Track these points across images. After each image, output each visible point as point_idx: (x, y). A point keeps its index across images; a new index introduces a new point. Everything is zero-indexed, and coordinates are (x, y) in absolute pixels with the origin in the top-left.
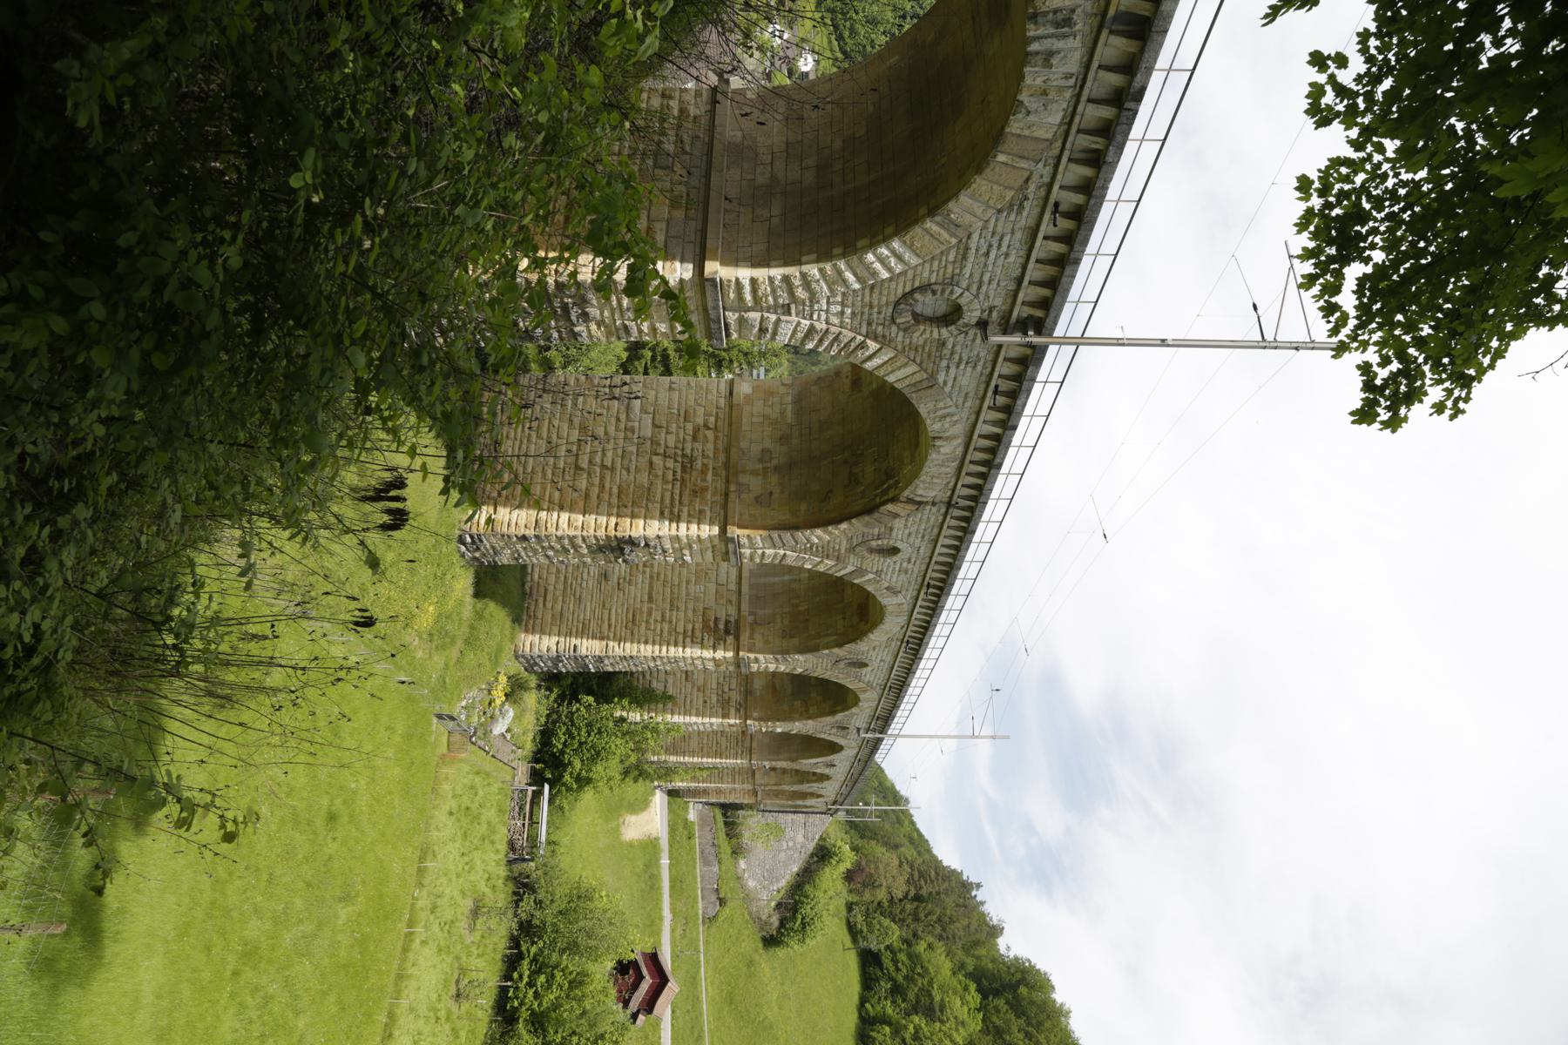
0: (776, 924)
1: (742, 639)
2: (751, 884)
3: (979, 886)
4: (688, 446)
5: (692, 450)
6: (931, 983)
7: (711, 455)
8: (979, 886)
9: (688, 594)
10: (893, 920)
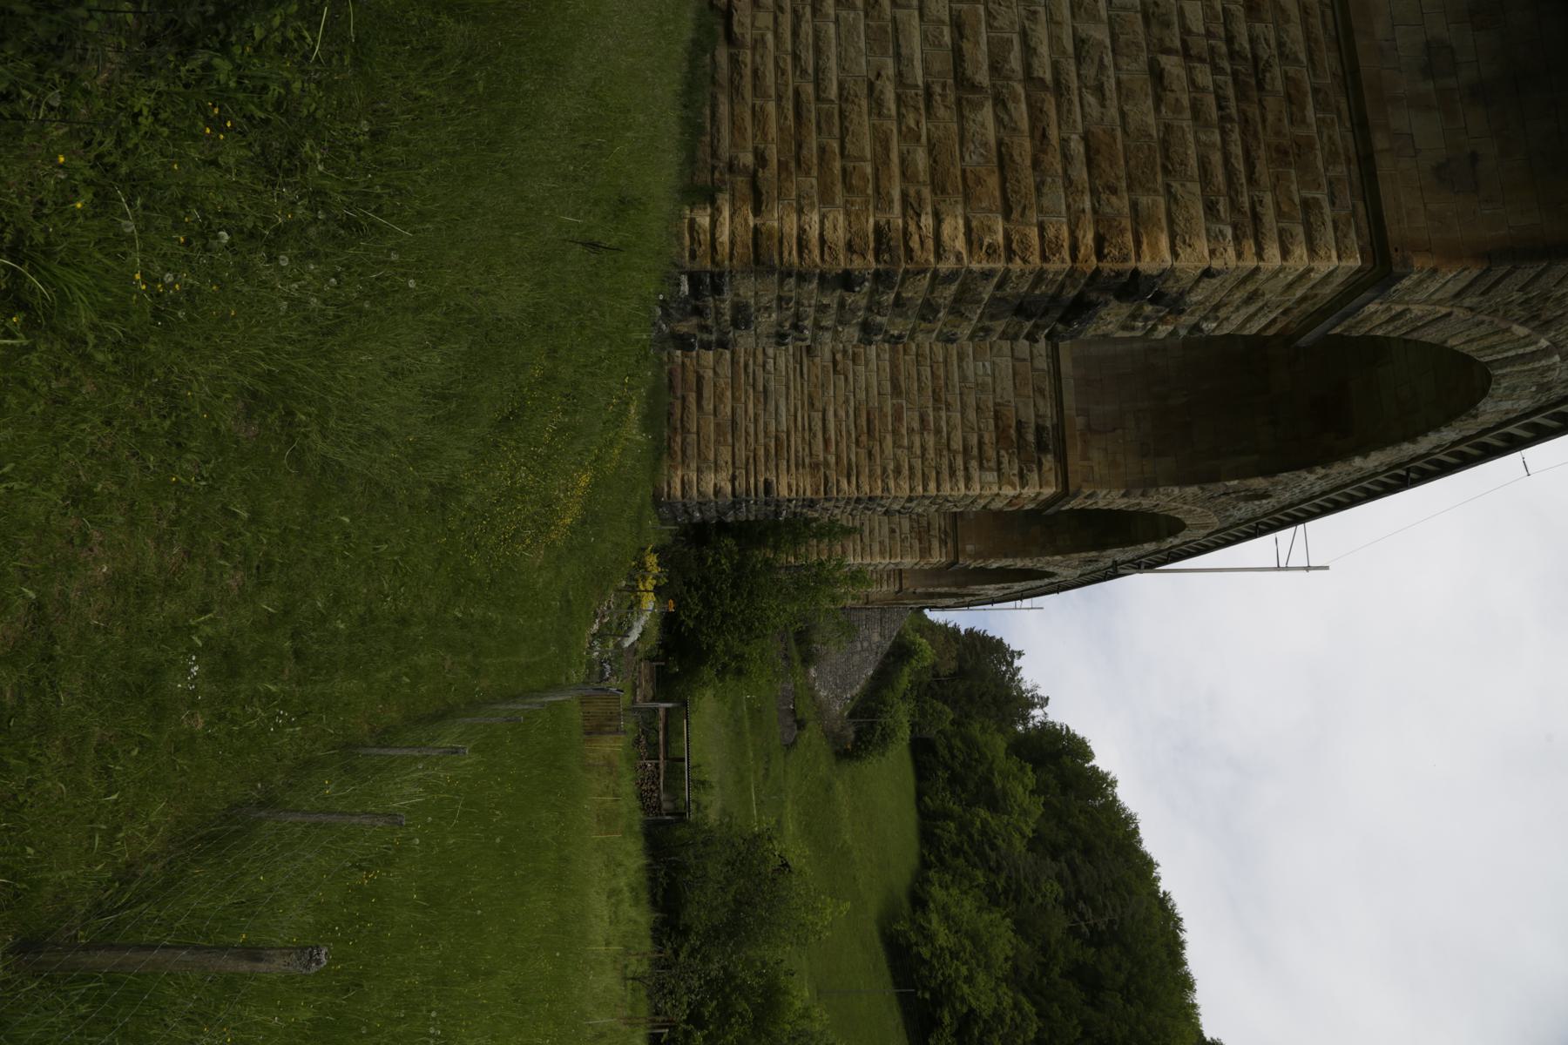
0: (853, 737)
1: (1070, 460)
2: (823, 694)
3: (1020, 654)
4: (1241, 29)
5: (1252, 40)
6: (990, 771)
7: (1303, 57)
8: (1020, 654)
9: (964, 378)
10: (945, 702)
